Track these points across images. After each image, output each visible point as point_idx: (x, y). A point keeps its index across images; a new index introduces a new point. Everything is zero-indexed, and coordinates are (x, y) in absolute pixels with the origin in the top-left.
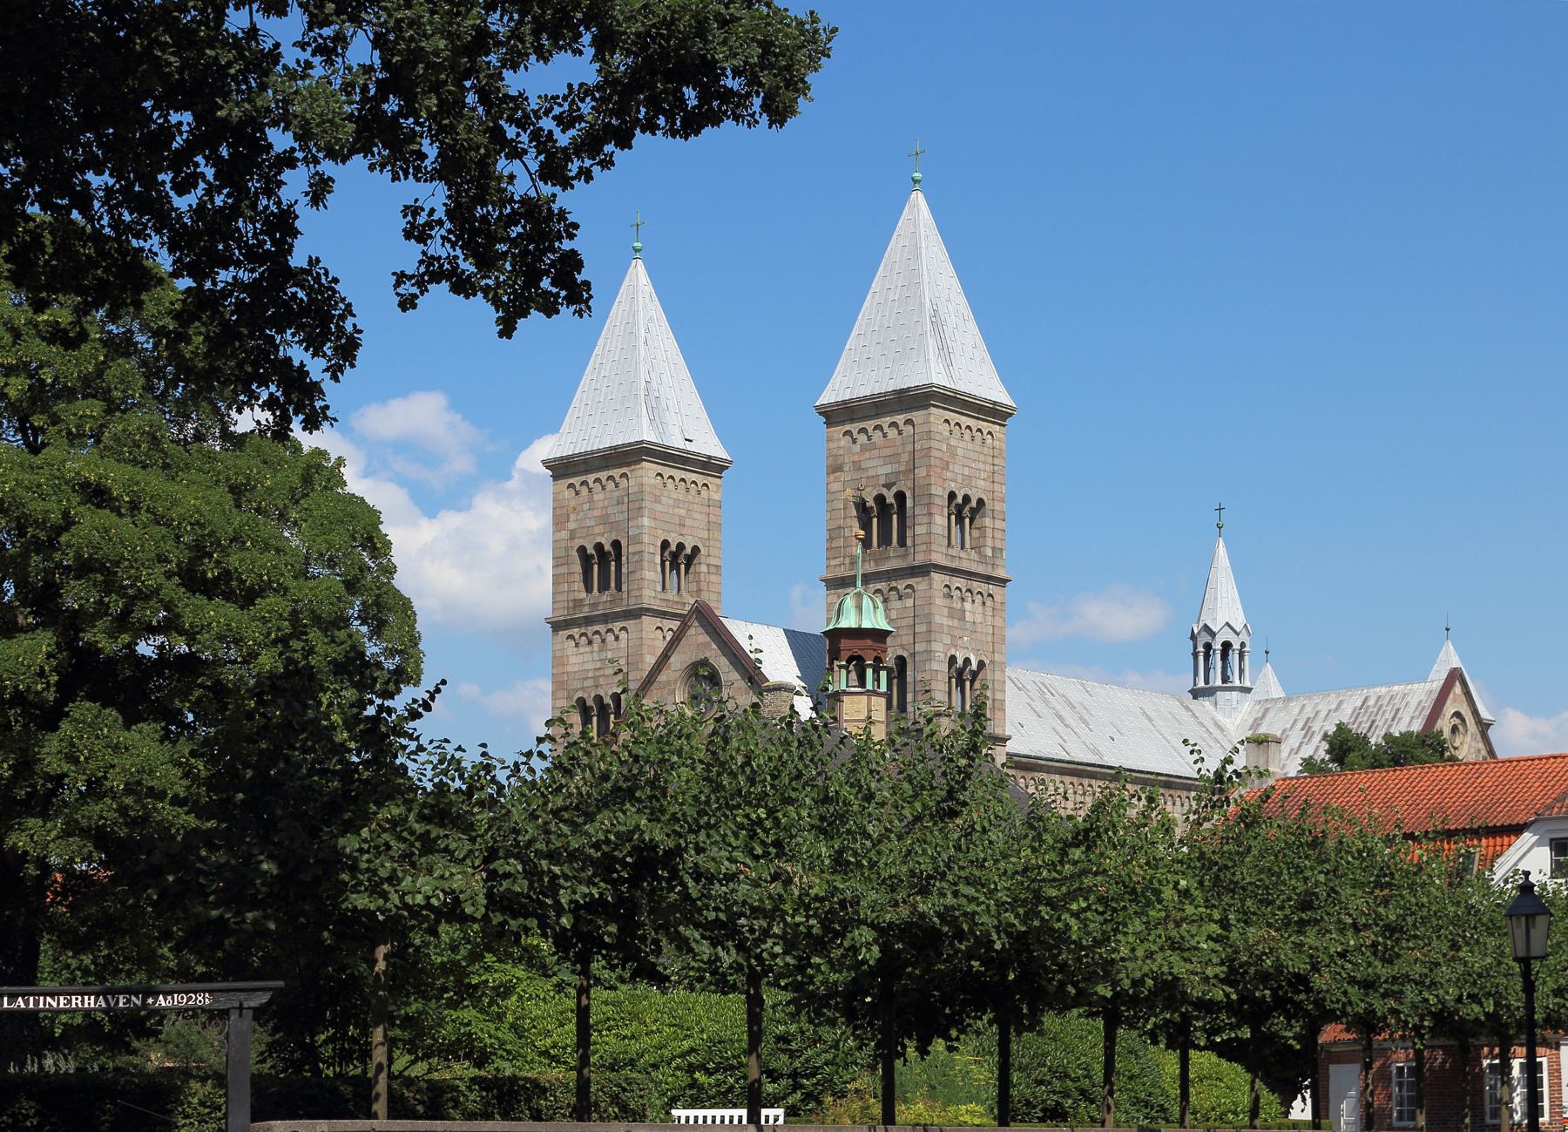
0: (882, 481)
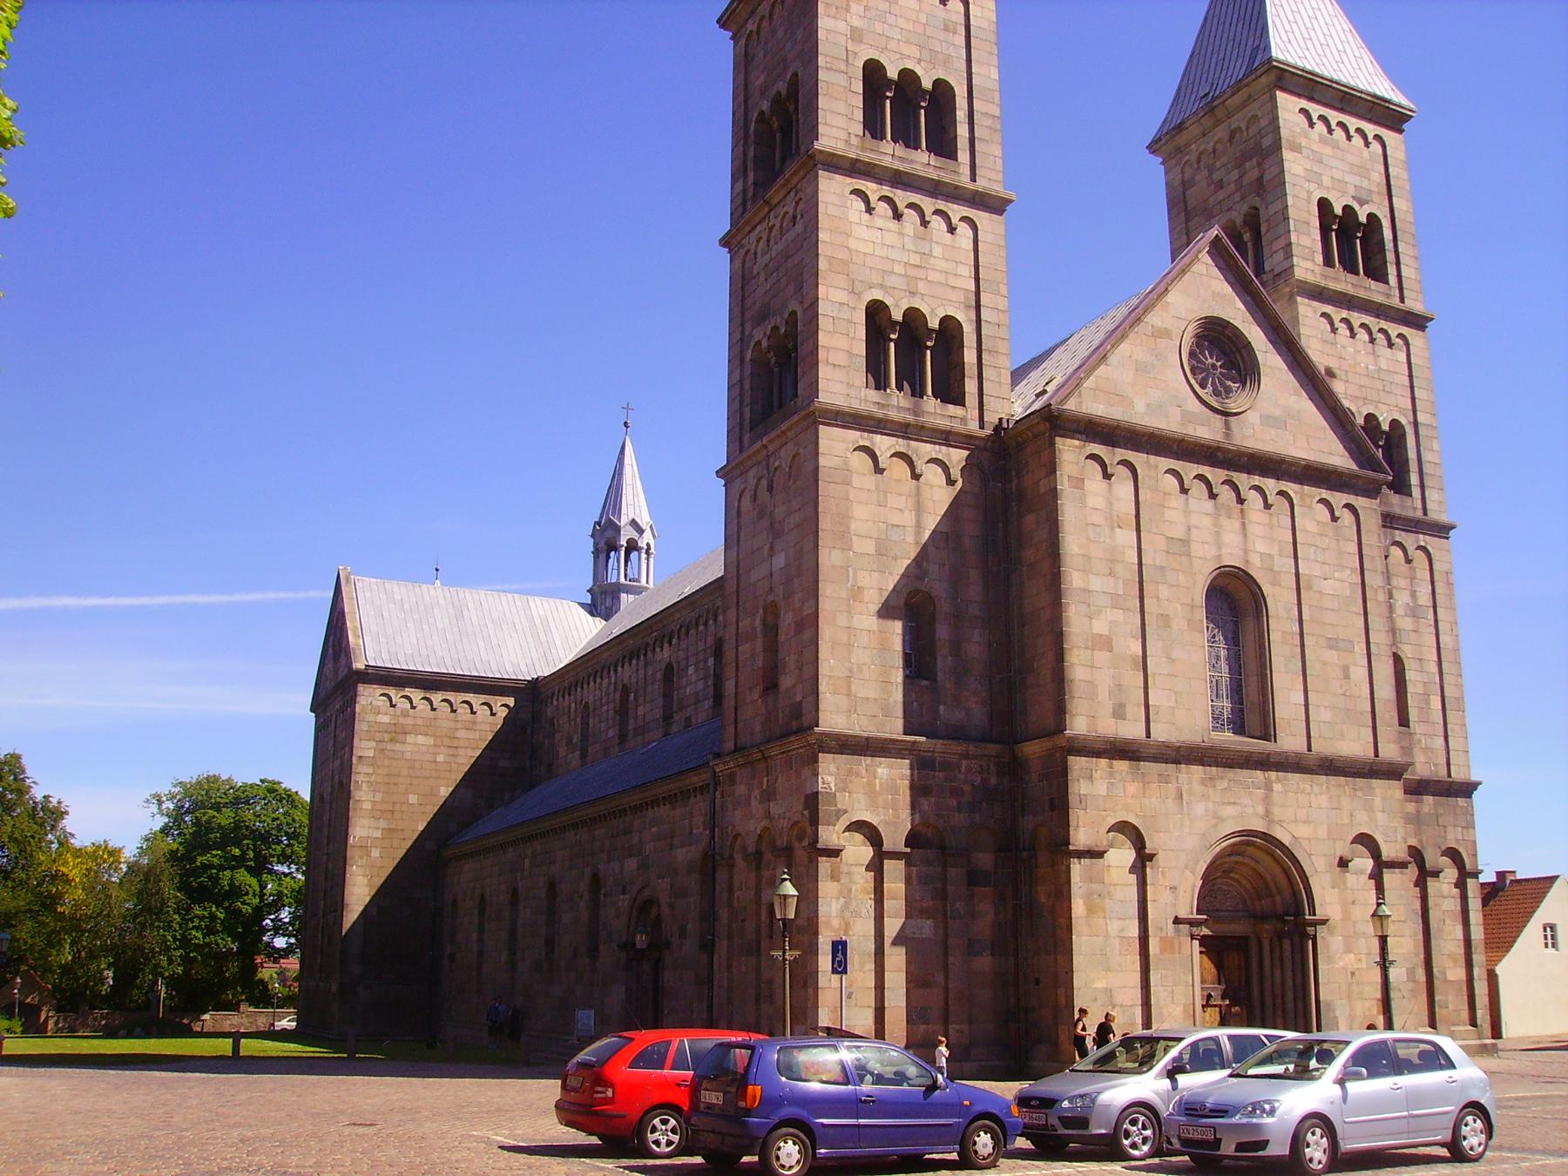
0: (1352, 191)
